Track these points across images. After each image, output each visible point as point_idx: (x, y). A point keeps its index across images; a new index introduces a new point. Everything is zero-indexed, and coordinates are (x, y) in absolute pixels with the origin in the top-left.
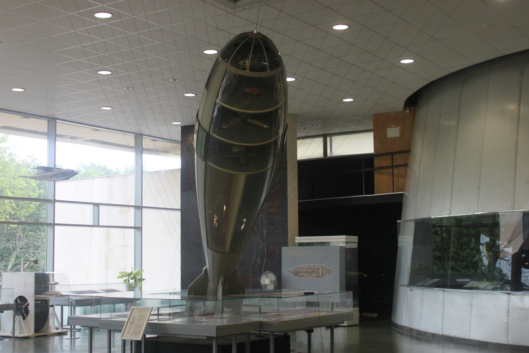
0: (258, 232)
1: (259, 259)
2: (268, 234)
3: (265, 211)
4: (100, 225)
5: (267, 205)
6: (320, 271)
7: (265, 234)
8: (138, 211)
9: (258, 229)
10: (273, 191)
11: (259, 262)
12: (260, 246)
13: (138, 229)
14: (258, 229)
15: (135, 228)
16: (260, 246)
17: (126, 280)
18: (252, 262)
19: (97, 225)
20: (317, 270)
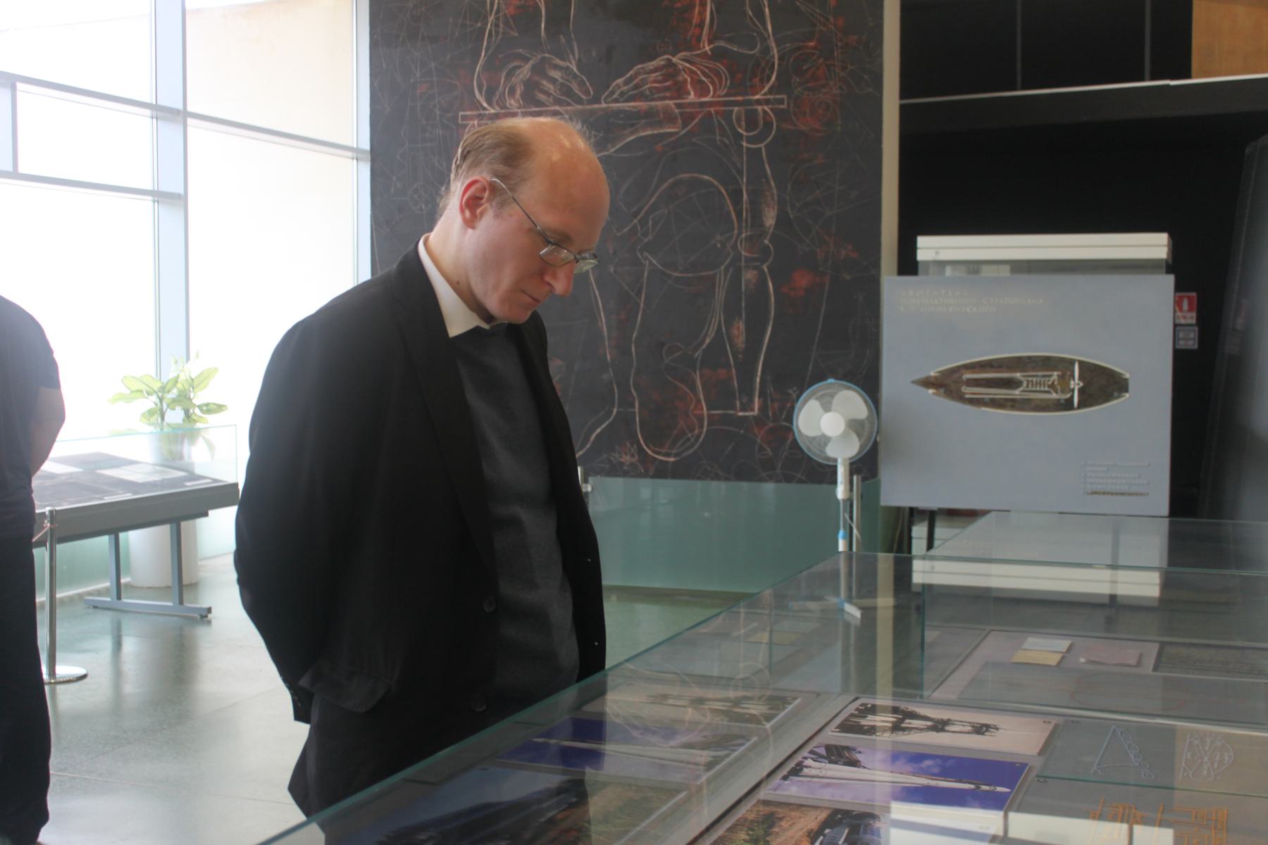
0: (739, 214)
1: (739, 330)
2: (782, 220)
3: (772, 123)
4: (22, 169)
5: (781, 102)
6: (1076, 384)
7: (770, 219)
8: (171, 131)
10: (812, 44)
11: (741, 341)
12: (749, 276)
15: (159, 196)
16: (749, 276)
17: (151, 413)
18: (708, 341)
19: (10, 169)
20: (1062, 377)
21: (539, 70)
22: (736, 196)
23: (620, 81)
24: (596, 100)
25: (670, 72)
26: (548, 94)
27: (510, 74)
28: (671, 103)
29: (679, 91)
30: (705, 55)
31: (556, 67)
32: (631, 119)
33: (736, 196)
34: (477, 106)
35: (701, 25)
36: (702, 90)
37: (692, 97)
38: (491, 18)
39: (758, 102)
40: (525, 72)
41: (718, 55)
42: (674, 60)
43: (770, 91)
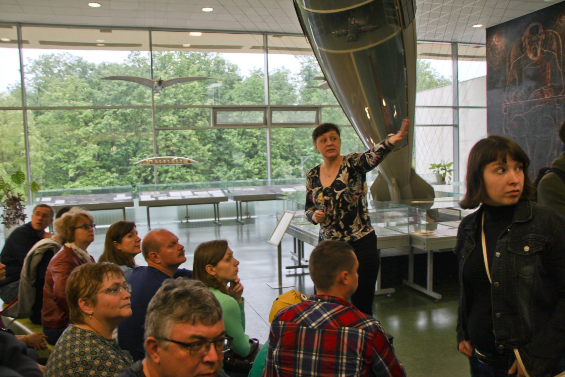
9: (555, 122)
13: (456, 126)
14: (555, 122)
21: (516, 94)
22: (555, 120)
23: (532, 94)
24: (527, 99)
25: (542, 92)
26: (518, 98)
27: (511, 95)
28: (542, 99)
29: (543, 96)
30: (549, 87)
31: (520, 92)
32: (534, 104)
33: (555, 120)
34: (505, 102)
35: (548, 79)
36: (548, 96)
37: (546, 97)
38: (508, 82)
39: (560, 97)
40: (514, 94)
41: (552, 86)
42: (543, 88)
43: (562, 94)
